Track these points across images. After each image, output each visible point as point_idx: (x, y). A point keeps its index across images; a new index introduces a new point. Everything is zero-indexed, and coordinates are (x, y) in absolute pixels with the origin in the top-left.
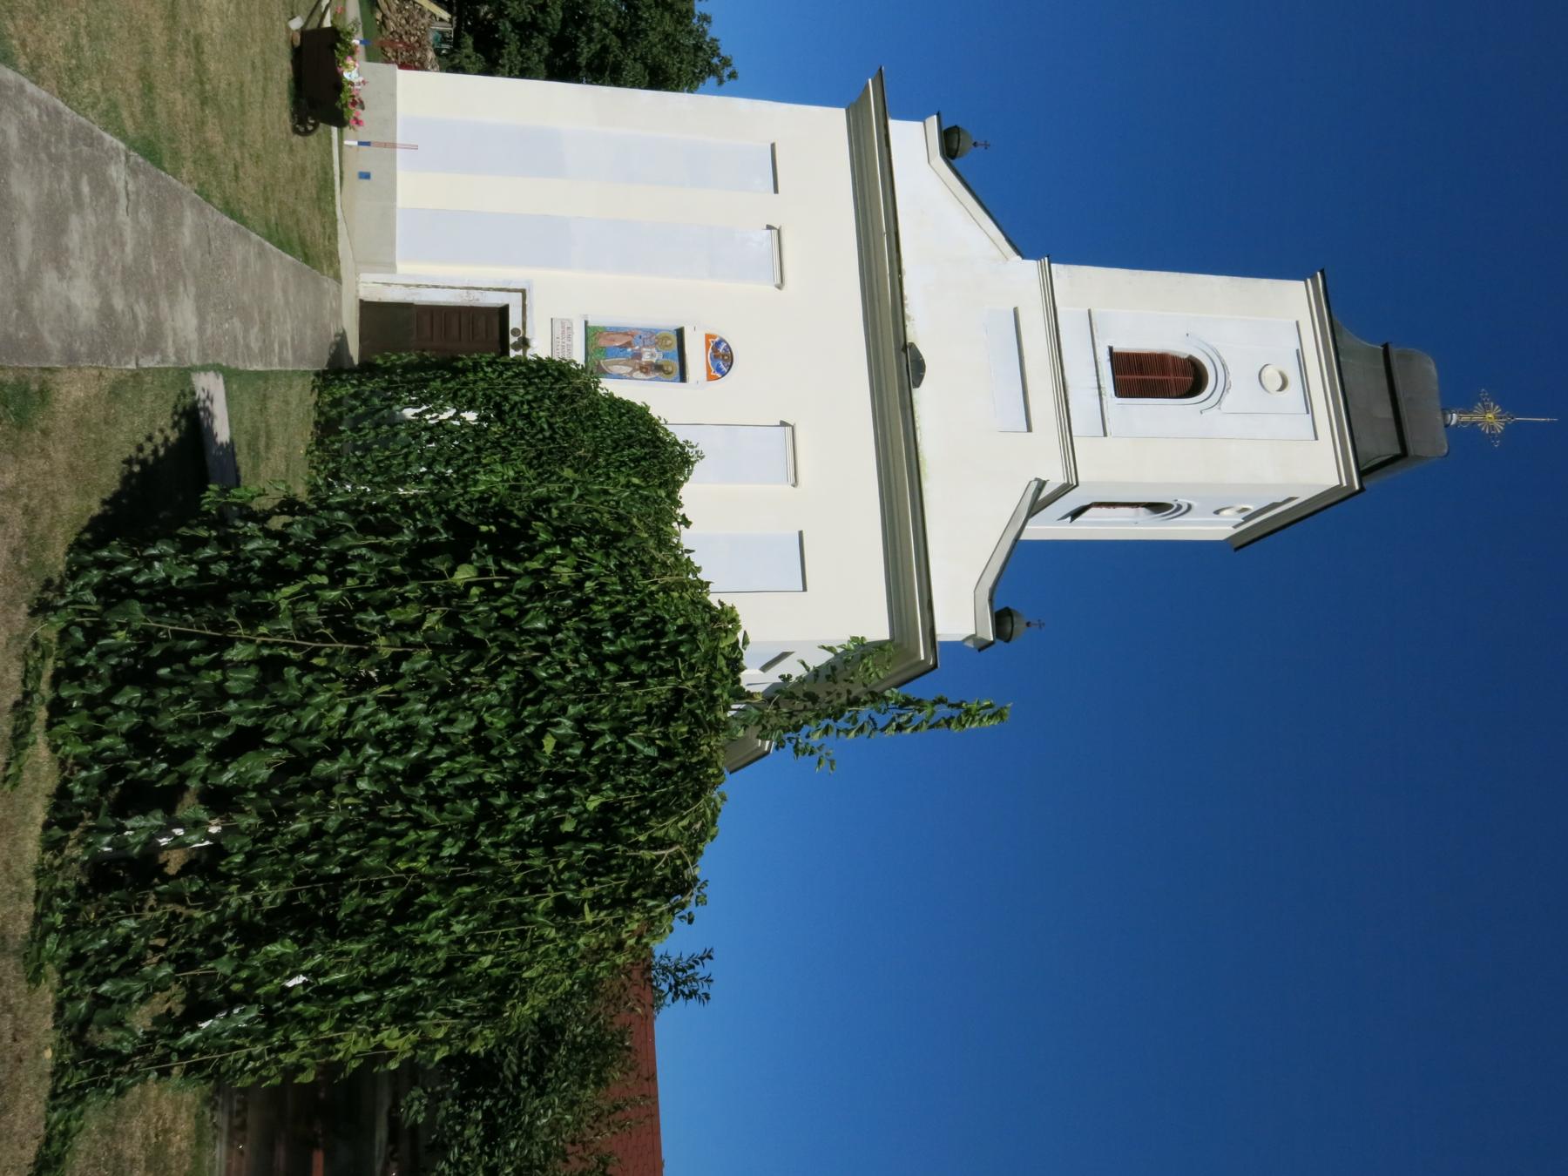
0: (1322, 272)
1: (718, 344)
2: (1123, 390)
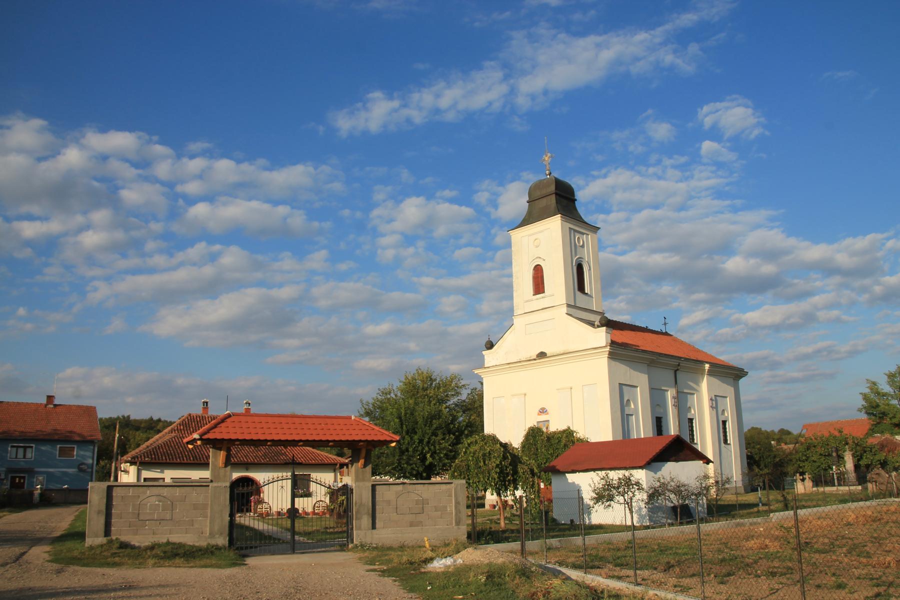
0: (508, 231)
1: (540, 412)
2: (543, 292)
